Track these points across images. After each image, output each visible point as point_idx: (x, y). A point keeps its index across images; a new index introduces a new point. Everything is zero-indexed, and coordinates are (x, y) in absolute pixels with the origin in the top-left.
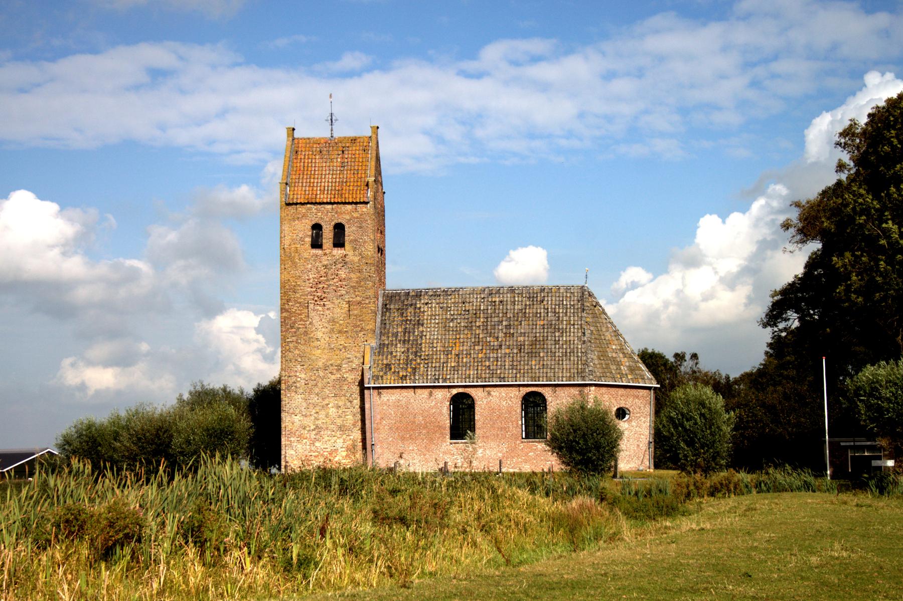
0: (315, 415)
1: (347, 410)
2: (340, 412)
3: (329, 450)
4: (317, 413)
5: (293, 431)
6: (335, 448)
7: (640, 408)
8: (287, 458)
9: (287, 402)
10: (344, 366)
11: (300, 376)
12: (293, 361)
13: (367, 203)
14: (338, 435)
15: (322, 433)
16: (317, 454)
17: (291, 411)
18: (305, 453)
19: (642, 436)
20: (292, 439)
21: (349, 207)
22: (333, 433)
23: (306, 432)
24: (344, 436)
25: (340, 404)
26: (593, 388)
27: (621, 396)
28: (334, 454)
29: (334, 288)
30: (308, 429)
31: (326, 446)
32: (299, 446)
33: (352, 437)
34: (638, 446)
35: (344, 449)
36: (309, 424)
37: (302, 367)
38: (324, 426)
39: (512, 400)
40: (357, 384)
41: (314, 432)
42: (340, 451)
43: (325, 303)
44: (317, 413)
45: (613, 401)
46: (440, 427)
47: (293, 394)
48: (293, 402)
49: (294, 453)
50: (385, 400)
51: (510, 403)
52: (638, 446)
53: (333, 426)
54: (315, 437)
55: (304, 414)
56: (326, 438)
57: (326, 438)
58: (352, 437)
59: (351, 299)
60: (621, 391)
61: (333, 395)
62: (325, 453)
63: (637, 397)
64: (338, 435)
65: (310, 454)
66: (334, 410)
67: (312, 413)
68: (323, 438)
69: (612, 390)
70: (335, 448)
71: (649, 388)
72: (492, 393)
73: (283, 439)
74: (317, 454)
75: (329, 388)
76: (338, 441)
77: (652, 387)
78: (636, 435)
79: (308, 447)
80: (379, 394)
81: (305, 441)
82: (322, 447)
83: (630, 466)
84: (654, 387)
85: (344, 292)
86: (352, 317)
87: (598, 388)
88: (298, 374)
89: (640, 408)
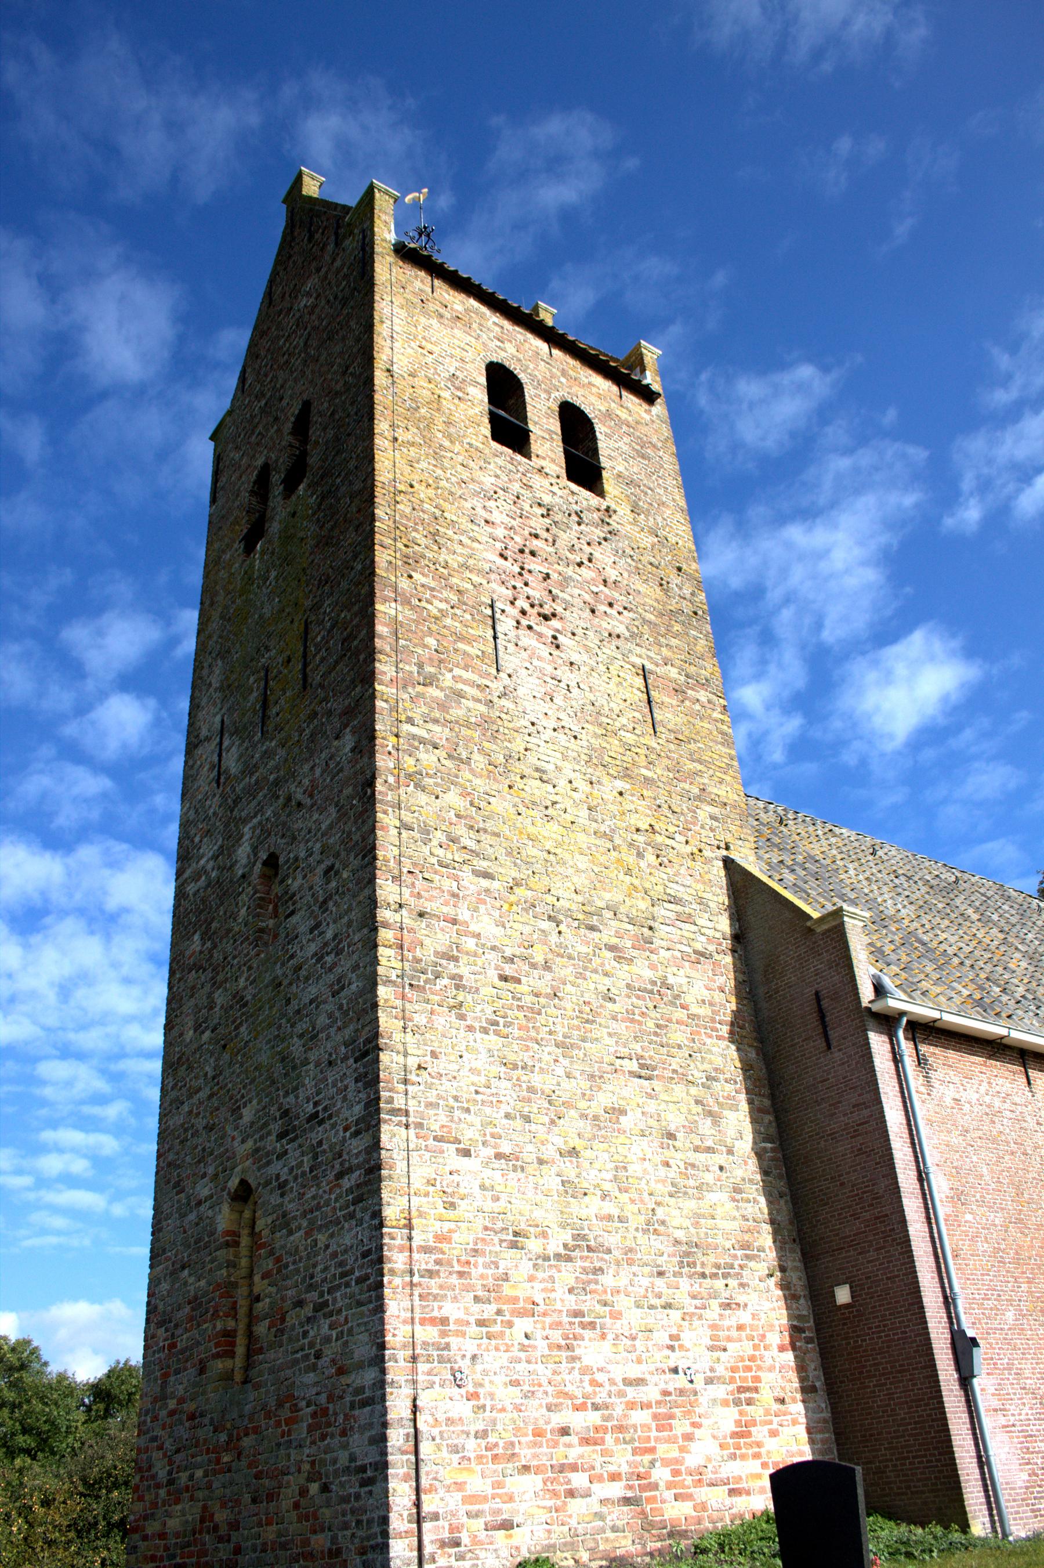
0: (569, 1169)
1: (701, 1158)
2: (677, 1159)
3: (651, 1393)
4: (574, 1152)
5: (454, 1251)
6: (681, 1381)
8: (425, 1448)
9: (412, 1062)
10: (662, 930)
11: (474, 927)
12: (439, 836)
14: (690, 1305)
15: (607, 1280)
16: (594, 1418)
17: (437, 1121)
18: (535, 1411)
20: (450, 1310)
22: (660, 1283)
23: (526, 1267)
24: (714, 1311)
25: (674, 1120)
28: (681, 1426)
30: (534, 1245)
31: (634, 1371)
32: (494, 1360)
33: (744, 1317)
35: (720, 1391)
36: (538, 1214)
37: (485, 883)
38: (612, 1240)
40: (725, 1030)
41: (567, 1275)
42: (703, 1400)
44: (574, 1152)
47: (443, 1020)
48: (440, 1065)
49: (463, 1409)
50: (948, 1101)
53: (656, 1243)
54: (571, 1302)
55: (506, 1148)
56: (633, 1318)
57: (633, 1318)
58: (744, 1317)
61: (634, 1066)
62: (640, 1417)
64: (690, 1305)
65: (558, 1419)
66: (647, 1147)
67: (549, 1152)
68: (616, 1316)
70: (681, 1381)
73: (396, 1307)
74: (594, 1418)
75: (613, 1024)
76: (687, 1338)
79: (544, 1372)
81: (523, 1325)
82: (618, 1373)
88: (464, 914)
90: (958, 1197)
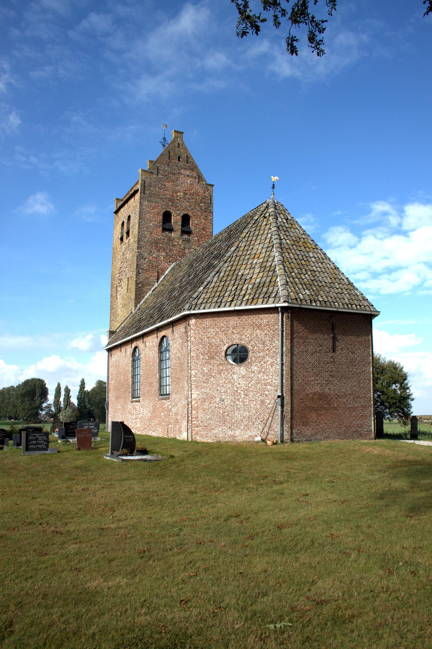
7: (264, 343)
13: (138, 190)
19: (268, 387)
21: (133, 199)
26: (193, 321)
27: (234, 328)
29: (124, 269)
34: (263, 402)
39: (155, 349)
43: (122, 283)
45: (222, 336)
46: (128, 384)
51: (153, 352)
52: (263, 402)
59: (129, 276)
60: (233, 320)
63: (259, 327)
69: (222, 321)
71: (274, 310)
72: (147, 343)
77: (277, 308)
78: (259, 386)
80: (111, 355)
83: (250, 434)
84: (282, 308)
85: (127, 271)
86: (129, 290)
87: (200, 321)
89: (264, 343)
90: (111, 380)
